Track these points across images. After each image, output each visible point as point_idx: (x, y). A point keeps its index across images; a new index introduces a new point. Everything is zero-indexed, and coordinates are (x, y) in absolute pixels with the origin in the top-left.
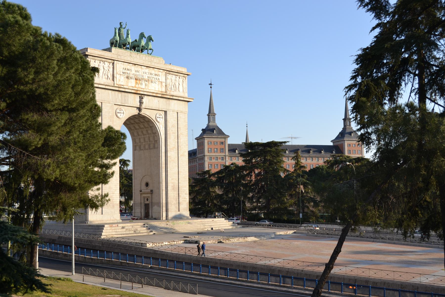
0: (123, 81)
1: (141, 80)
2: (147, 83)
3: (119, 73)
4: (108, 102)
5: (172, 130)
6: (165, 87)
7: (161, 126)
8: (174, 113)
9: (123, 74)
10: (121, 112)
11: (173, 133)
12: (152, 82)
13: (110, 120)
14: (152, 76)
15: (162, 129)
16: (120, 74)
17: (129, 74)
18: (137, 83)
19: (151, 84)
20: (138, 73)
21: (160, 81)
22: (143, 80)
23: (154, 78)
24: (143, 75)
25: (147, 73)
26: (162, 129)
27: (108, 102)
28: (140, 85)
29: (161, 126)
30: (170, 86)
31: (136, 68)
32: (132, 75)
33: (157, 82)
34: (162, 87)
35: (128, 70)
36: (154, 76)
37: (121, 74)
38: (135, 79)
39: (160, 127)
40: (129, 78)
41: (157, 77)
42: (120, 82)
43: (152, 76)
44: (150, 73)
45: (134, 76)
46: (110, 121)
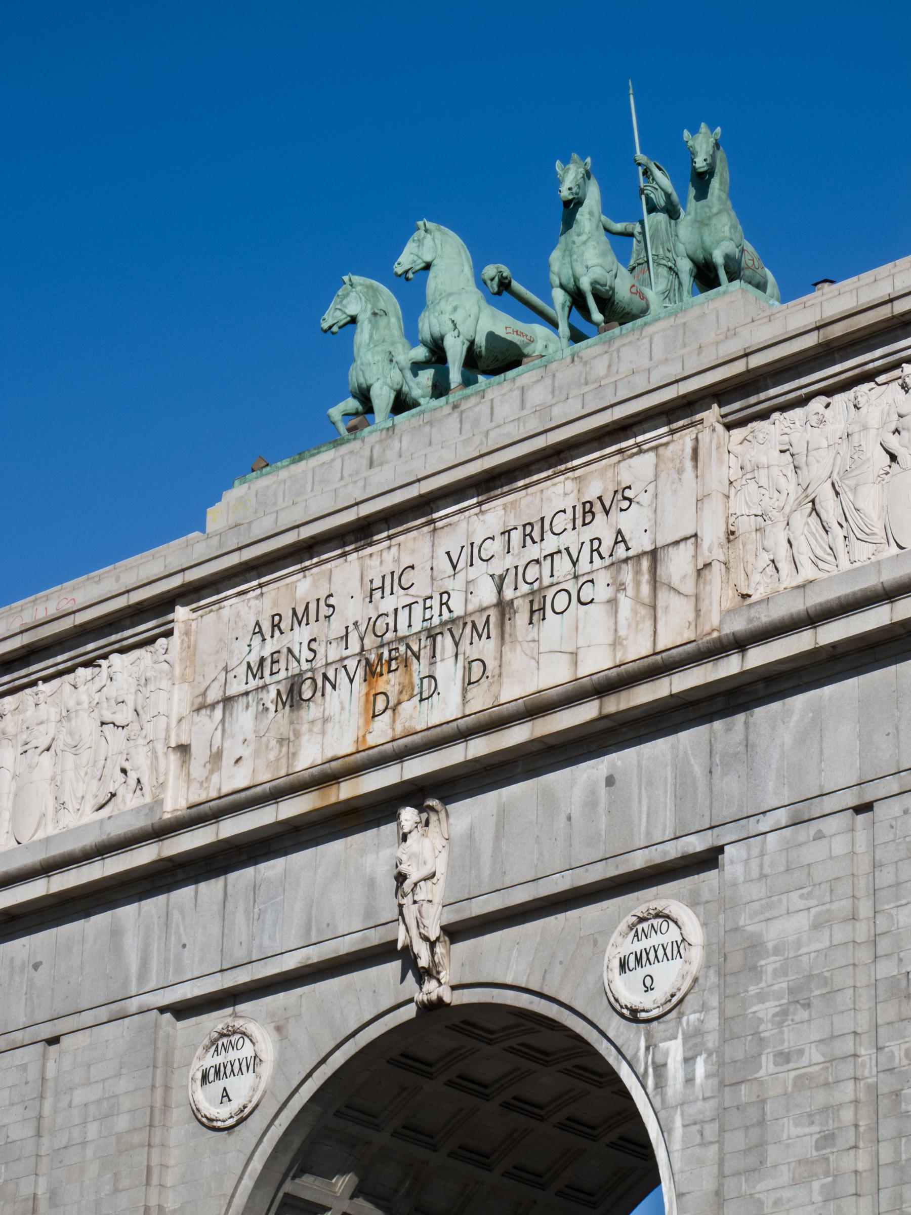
0: (246, 752)
1: (425, 654)
2: (486, 648)
3: (214, 695)
4: (103, 1014)
5: (784, 1057)
6: (688, 587)
7: (674, 1051)
8: (819, 836)
9: (253, 683)
10: (233, 1055)
11: (803, 1083)
12: (537, 612)
13: (116, 1176)
14: (551, 543)
15: (689, 1080)
16: (227, 701)
17: (306, 654)
18: (381, 703)
19: (533, 633)
20: (388, 604)
21: (640, 543)
22: (445, 643)
23: (563, 565)
24: (449, 585)
25: (495, 547)
26: (689, 1080)
27: (103, 1014)
28: (407, 707)
29: (674, 1051)
30: (777, 536)
31: (375, 561)
32: (334, 653)
33: (603, 578)
34: (664, 596)
35: (300, 618)
36: (570, 539)
37: (233, 690)
38: (360, 673)
39: (660, 1068)
40: (307, 695)
41: (602, 528)
42: (215, 778)
43: (551, 543)
44: (516, 536)
45: (354, 646)
46: (116, 1190)
